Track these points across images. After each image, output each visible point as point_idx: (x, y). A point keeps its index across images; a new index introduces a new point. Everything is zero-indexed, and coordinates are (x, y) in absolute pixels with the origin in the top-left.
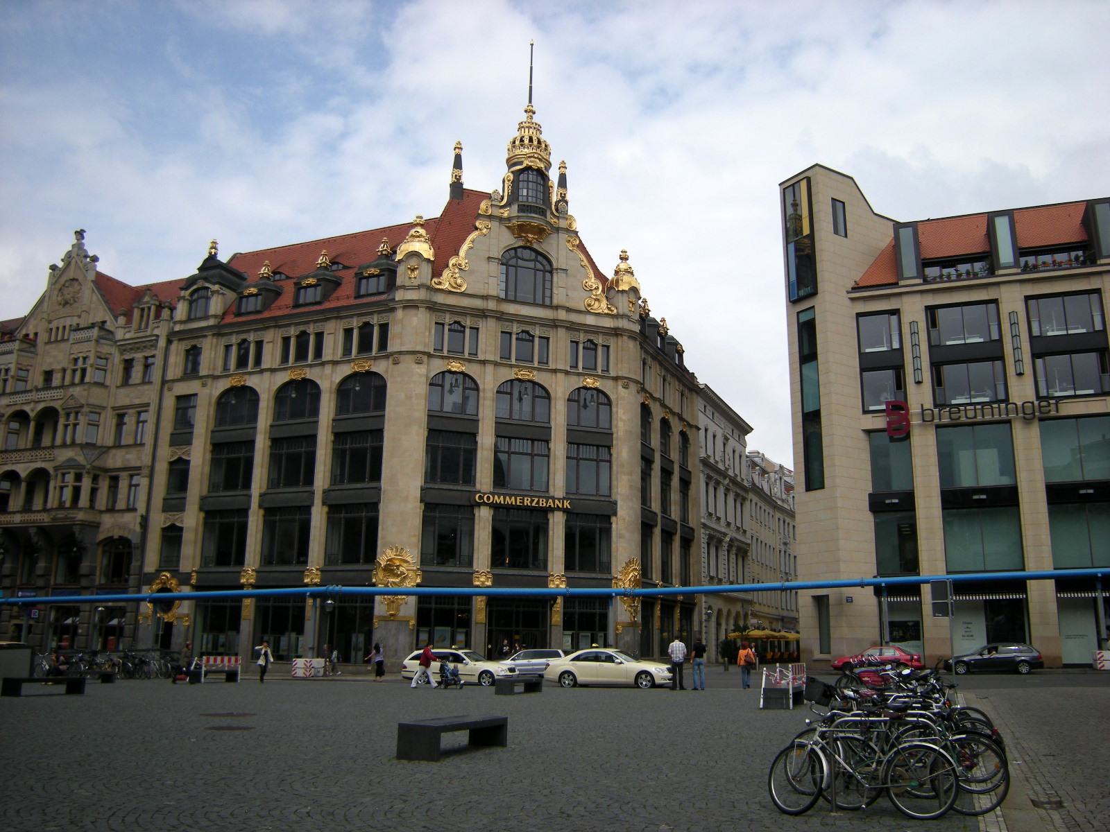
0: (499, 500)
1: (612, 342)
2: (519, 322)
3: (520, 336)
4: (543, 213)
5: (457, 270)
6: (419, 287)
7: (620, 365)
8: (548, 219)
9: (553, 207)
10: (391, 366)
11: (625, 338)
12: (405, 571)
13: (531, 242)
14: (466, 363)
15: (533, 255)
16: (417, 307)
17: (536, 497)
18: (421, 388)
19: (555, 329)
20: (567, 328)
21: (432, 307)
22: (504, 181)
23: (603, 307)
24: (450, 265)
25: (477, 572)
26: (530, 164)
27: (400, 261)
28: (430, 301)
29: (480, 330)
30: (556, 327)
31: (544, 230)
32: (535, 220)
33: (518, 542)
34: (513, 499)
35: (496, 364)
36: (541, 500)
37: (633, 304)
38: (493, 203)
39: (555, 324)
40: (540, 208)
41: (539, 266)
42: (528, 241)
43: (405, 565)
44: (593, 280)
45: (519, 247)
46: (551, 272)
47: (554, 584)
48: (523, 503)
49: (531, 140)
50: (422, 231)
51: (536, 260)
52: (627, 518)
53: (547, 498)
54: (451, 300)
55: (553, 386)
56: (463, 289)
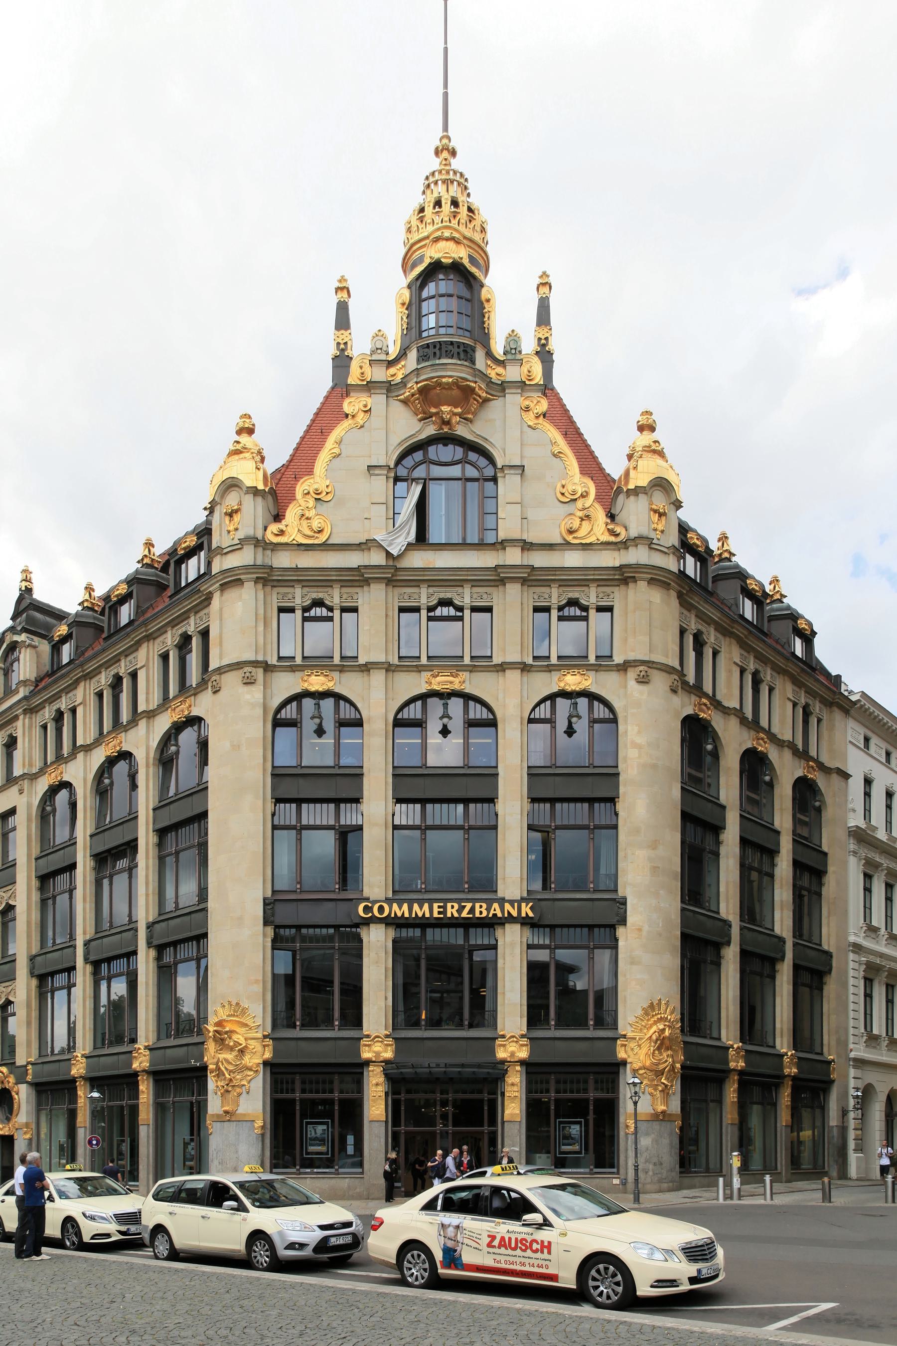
0: (401, 911)
2: (431, 583)
5: (311, 503)
11: (642, 585)
13: (448, 423)
14: (336, 675)
15: (459, 452)
17: (468, 900)
18: (256, 728)
19: (501, 588)
20: (524, 582)
21: (267, 578)
24: (299, 494)
25: (368, 1036)
30: (502, 582)
33: (441, 977)
34: (426, 906)
35: (389, 668)
36: (477, 905)
37: (661, 515)
39: (498, 578)
43: (242, 1030)
47: (505, 1051)
48: (444, 912)
52: (646, 928)
53: (489, 903)
55: (501, 696)
56: (322, 538)
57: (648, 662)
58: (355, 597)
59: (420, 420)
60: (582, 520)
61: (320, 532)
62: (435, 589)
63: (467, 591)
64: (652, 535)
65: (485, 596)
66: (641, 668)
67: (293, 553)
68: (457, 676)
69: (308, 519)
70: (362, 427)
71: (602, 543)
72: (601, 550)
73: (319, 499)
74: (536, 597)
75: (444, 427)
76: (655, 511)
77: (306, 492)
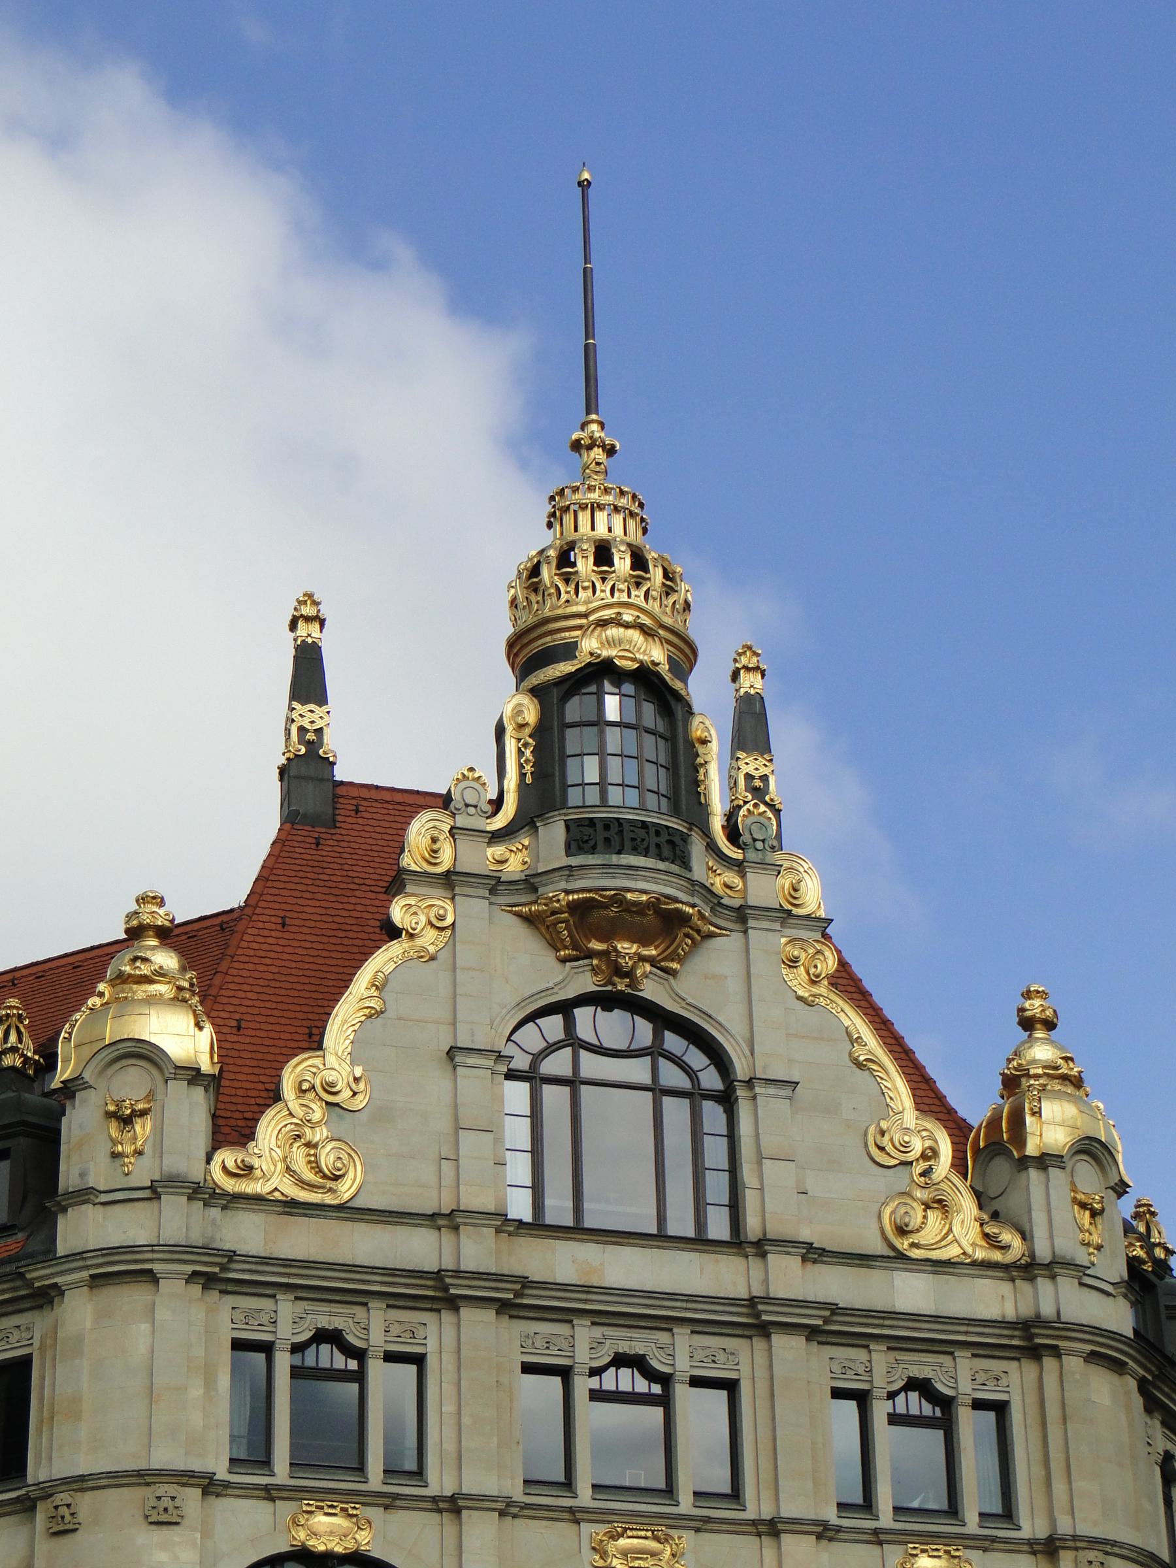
1: (1015, 1381)
2: (599, 1318)
3: (609, 1381)
4: (673, 849)
6: (154, 1192)
7: (1059, 1487)
8: (699, 871)
9: (717, 824)
10: (43, 1546)
11: (1073, 1363)
14: (375, 1514)
16: (151, 1277)
20: (813, 1333)
22: (500, 731)
23: (962, 1230)
26: (605, 653)
27: (69, 1090)
28: (207, 1249)
29: (431, 1362)
31: (684, 919)
32: (643, 880)
37: (1094, 1214)
38: (461, 821)
39: (756, 1320)
40: (659, 830)
41: (672, 1076)
42: (619, 971)
44: (910, 1117)
45: (584, 1000)
46: (726, 1099)
49: (603, 554)
50: (167, 960)
51: (655, 1052)
54: (302, 1241)
56: (346, 1190)
57: (1105, 1542)
58: (420, 1333)
59: (564, 961)
60: (927, 1207)
61: (337, 1178)
62: (609, 1331)
63: (683, 1339)
64: (1082, 1258)
65: (721, 1357)
66: (1092, 1555)
67: (273, 1218)
68: (666, 1540)
69: (308, 1145)
70: (433, 958)
71: (974, 1264)
72: (972, 1276)
73: (337, 1105)
74: (837, 1368)
75: (616, 979)
76: (1083, 1206)
77: (305, 1086)
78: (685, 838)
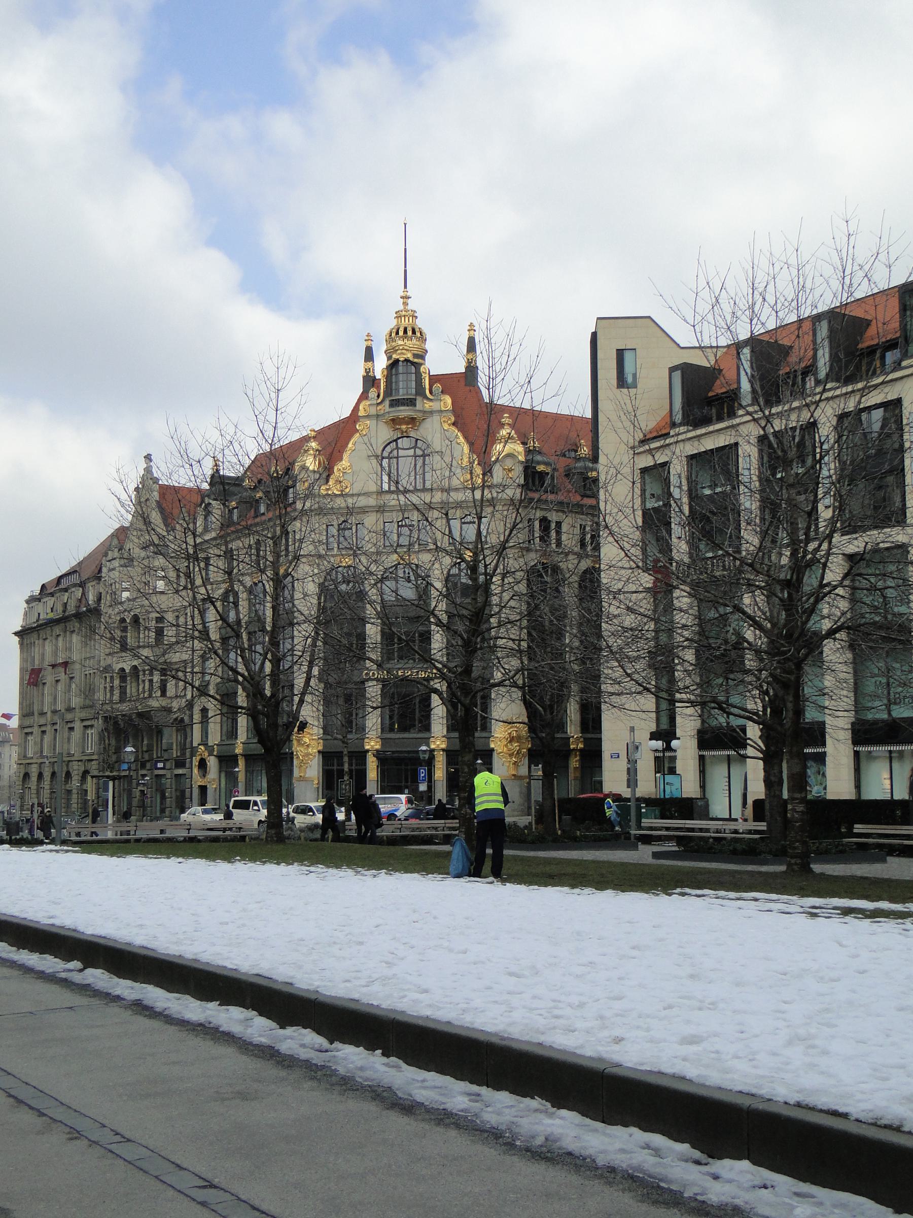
4: (411, 402)
9: (427, 392)
12: (307, 740)
32: (404, 412)
78: (415, 400)
